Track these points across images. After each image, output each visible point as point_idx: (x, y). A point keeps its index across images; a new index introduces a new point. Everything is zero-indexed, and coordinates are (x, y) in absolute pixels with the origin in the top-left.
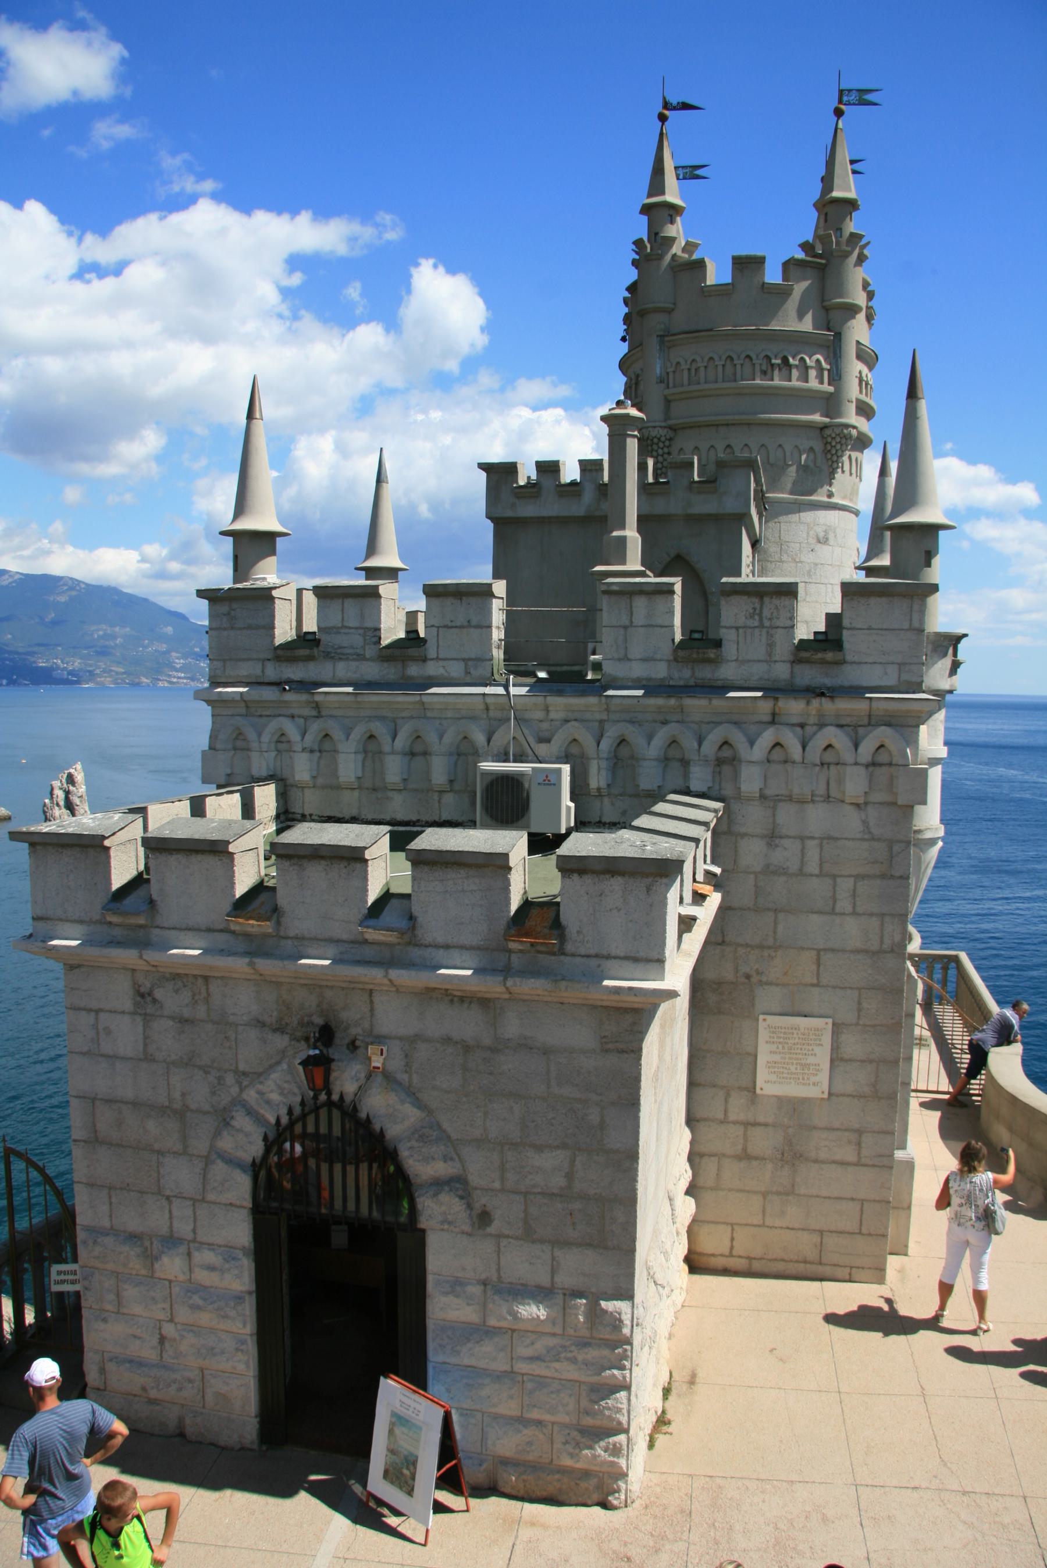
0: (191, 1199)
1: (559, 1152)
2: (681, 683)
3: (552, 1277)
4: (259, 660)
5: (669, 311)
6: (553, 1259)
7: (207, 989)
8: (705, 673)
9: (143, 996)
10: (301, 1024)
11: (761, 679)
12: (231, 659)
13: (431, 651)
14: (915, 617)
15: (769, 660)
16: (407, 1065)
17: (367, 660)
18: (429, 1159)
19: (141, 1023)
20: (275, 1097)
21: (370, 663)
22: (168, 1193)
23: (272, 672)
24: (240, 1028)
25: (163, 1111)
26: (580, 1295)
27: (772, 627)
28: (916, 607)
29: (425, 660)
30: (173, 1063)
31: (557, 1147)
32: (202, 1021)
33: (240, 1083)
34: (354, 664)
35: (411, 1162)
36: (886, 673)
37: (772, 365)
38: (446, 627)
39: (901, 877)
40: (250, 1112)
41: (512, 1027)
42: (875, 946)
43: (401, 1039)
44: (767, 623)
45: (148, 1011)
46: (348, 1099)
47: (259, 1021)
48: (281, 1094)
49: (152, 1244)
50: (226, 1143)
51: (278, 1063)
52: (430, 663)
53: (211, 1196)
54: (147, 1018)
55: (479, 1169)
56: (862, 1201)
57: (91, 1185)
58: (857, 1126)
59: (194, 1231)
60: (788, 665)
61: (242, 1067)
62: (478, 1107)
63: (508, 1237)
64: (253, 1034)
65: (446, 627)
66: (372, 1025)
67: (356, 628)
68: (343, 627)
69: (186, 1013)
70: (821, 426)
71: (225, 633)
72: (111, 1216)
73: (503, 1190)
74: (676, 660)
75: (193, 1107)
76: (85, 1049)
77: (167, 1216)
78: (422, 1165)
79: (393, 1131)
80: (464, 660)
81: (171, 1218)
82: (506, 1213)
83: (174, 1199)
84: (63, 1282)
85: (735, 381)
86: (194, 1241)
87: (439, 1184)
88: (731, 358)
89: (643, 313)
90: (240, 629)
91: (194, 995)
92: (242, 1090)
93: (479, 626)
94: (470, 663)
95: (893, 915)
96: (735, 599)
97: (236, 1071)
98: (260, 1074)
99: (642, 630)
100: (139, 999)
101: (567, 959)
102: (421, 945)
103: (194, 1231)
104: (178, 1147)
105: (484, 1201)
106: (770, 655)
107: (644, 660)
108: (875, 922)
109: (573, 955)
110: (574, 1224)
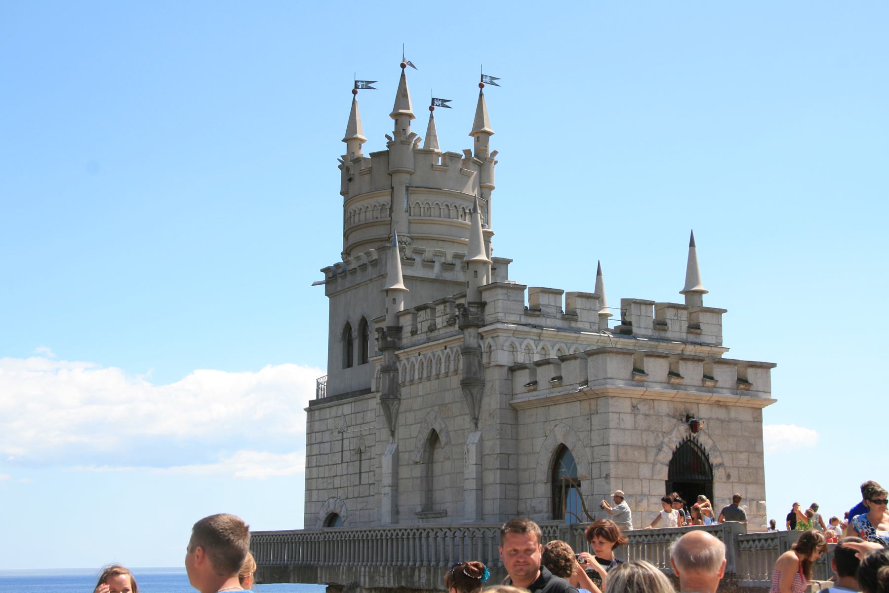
5: (411, 174)
8: (663, 334)
15: (680, 332)
18: (716, 457)
23: (524, 320)
26: (753, 500)
29: (577, 321)
53: (655, 477)
54: (635, 415)
55: (727, 460)
64: (666, 419)
69: (647, 413)
78: (714, 460)
79: (707, 448)
82: (734, 473)
104: (644, 460)
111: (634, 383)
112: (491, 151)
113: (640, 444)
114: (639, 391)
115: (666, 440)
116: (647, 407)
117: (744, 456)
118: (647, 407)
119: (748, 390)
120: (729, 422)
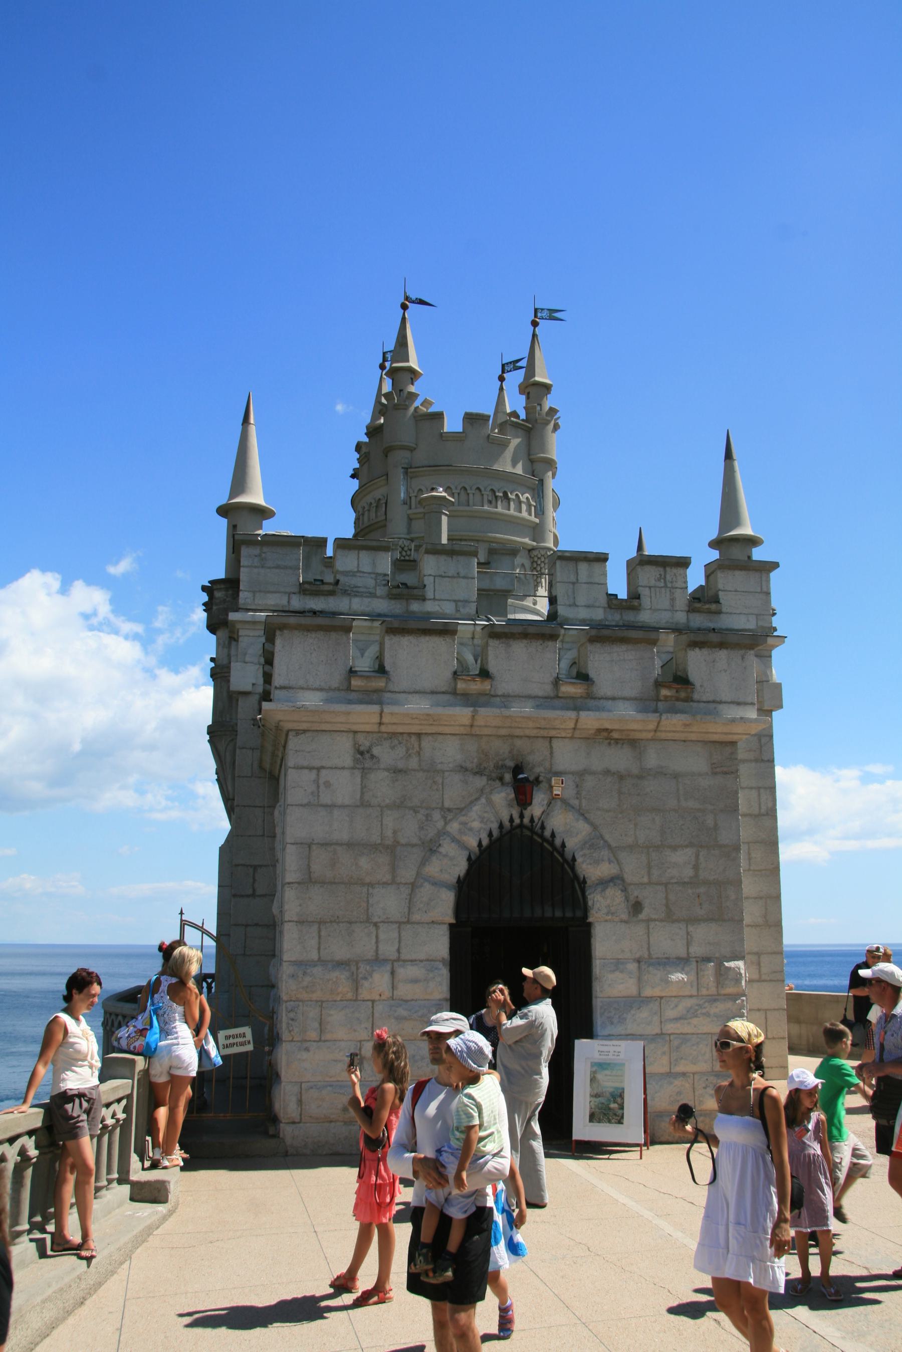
0: (396, 922)
1: (688, 850)
2: (614, 623)
3: (688, 949)
4: (285, 593)
5: (412, 450)
6: (688, 933)
7: (420, 745)
8: (630, 617)
9: (361, 753)
10: (497, 767)
11: (667, 622)
12: (260, 591)
13: (429, 594)
14: (764, 583)
15: (672, 609)
16: (578, 793)
17: (378, 597)
18: (597, 862)
19: (359, 776)
20: (476, 825)
21: (381, 600)
22: (376, 919)
24: (447, 774)
25: (374, 848)
26: (709, 960)
27: (673, 588)
28: (764, 578)
29: (424, 599)
30: (387, 806)
31: (686, 846)
32: (414, 770)
33: (444, 818)
34: (366, 600)
35: (584, 866)
36: (748, 621)
37: (496, 497)
38: (441, 576)
39: (768, 761)
40: (454, 840)
41: (652, 760)
42: (756, 812)
43: (573, 773)
44: (669, 585)
45: (366, 765)
46: (536, 820)
47: (462, 767)
48: (482, 822)
49: (358, 969)
50: (434, 868)
51: (477, 799)
52: (428, 603)
53: (416, 917)
54: (365, 772)
55: (633, 868)
56: (766, 1010)
57: (300, 922)
58: (756, 950)
59: (398, 951)
60: (685, 613)
61: (447, 804)
62: (630, 821)
63: (655, 920)
64: (457, 778)
65: (441, 576)
66: (551, 765)
67: (369, 573)
68: (358, 571)
69: (400, 765)
70: (530, 548)
71: (256, 570)
72: (319, 949)
73: (650, 883)
74: (610, 607)
75: (403, 841)
76: (305, 801)
77: (374, 941)
78: (592, 869)
79: (572, 844)
80: (455, 601)
81: (377, 942)
82: (653, 900)
83: (381, 925)
84: (232, 1045)
85: (468, 505)
86: (398, 960)
87: (604, 883)
88: (465, 489)
89: (387, 451)
90: (269, 568)
91: (408, 750)
92: (446, 824)
93: (464, 577)
94: (459, 604)
95: (765, 788)
96: (648, 568)
97: (442, 809)
98: (461, 810)
99: (585, 586)
100: (359, 756)
101: (694, 705)
102: (595, 698)
103: (398, 951)
105: (636, 894)
106: (673, 606)
107: (588, 606)
108: (754, 793)
109: (699, 702)
110: (701, 904)
111: (353, 696)
112: (546, 407)
113: (375, 838)
114: (364, 716)
115: (454, 827)
116: (401, 751)
117: (682, 857)
118: (401, 751)
119: (688, 699)
120: (640, 777)
